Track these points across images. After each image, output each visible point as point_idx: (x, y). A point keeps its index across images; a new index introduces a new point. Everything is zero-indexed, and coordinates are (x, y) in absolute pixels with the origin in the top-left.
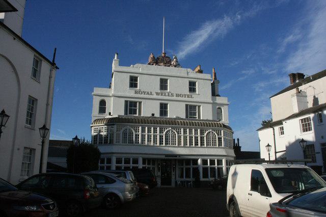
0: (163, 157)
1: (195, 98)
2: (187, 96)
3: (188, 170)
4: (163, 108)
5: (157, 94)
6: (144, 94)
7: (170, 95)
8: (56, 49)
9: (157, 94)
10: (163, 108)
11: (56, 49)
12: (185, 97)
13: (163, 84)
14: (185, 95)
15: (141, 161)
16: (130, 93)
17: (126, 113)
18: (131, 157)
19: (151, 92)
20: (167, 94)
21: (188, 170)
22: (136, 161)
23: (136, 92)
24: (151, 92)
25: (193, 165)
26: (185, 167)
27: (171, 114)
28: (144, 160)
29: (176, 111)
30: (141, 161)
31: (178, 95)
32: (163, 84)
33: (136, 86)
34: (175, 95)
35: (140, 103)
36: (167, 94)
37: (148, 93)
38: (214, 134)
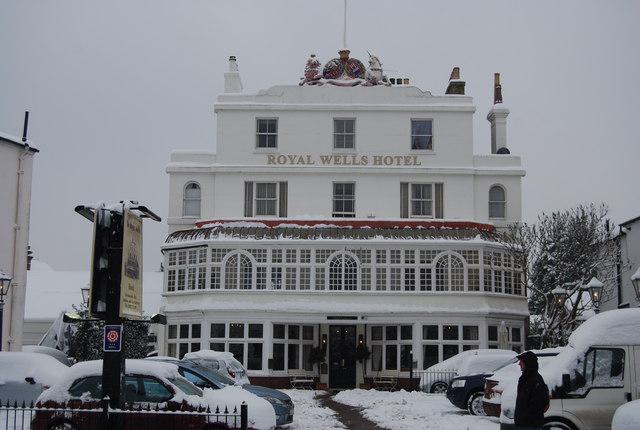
0: (324, 320)
1: (428, 166)
2: (402, 161)
3: (392, 350)
4: (344, 195)
5: (325, 160)
6: (292, 163)
7: (358, 159)
8: (27, 113)
9: (325, 160)
10: (344, 195)
11: (27, 113)
12: (398, 164)
13: (344, 133)
14: (398, 158)
15: (268, 332)
16: (259, 164)
17: (248, 213)
18: (246, 321)
19: (309, 157)
20: (349, 159)
21: (392, 350)
22: (256, 330)
23: (271, 160)
24: (309, 157)
25: (402, 339)
26: (385, 343)
27: (366, 209)
28: (279, 330)
29: (378, 202)
30: (268, 332)
31: (378, 160)
32: (344, 133)
33: (273, 143)
34: (371, 160)
35: (284, 185)
36: (349, 159)
37: (301, 160)
38: (458, 260)
